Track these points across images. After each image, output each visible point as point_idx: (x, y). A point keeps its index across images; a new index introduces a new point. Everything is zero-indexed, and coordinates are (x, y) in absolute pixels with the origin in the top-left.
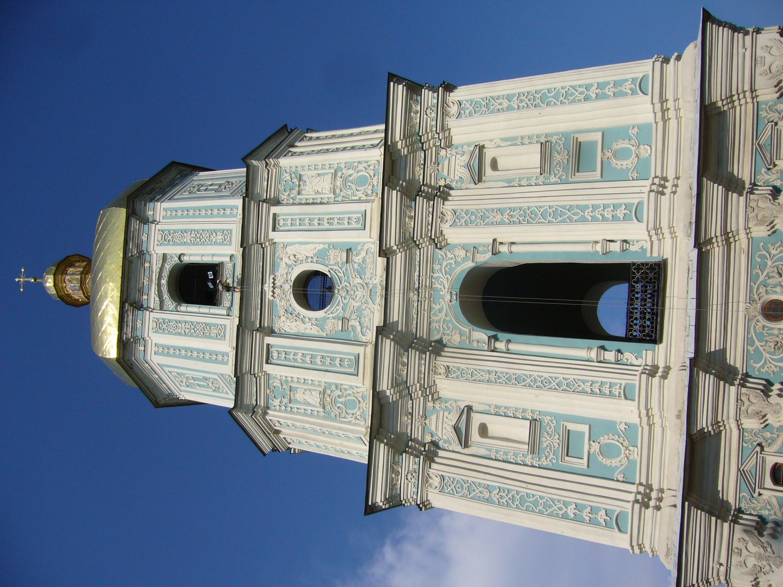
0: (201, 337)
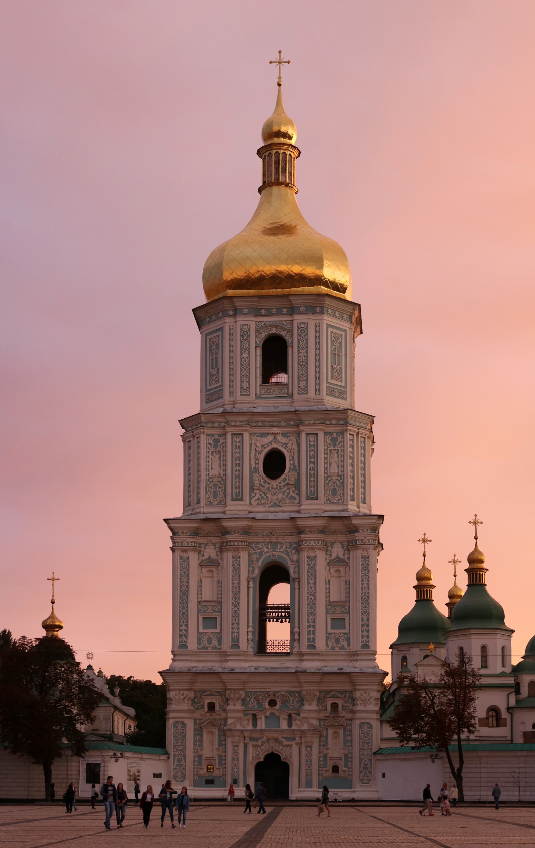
0: (241, 374)
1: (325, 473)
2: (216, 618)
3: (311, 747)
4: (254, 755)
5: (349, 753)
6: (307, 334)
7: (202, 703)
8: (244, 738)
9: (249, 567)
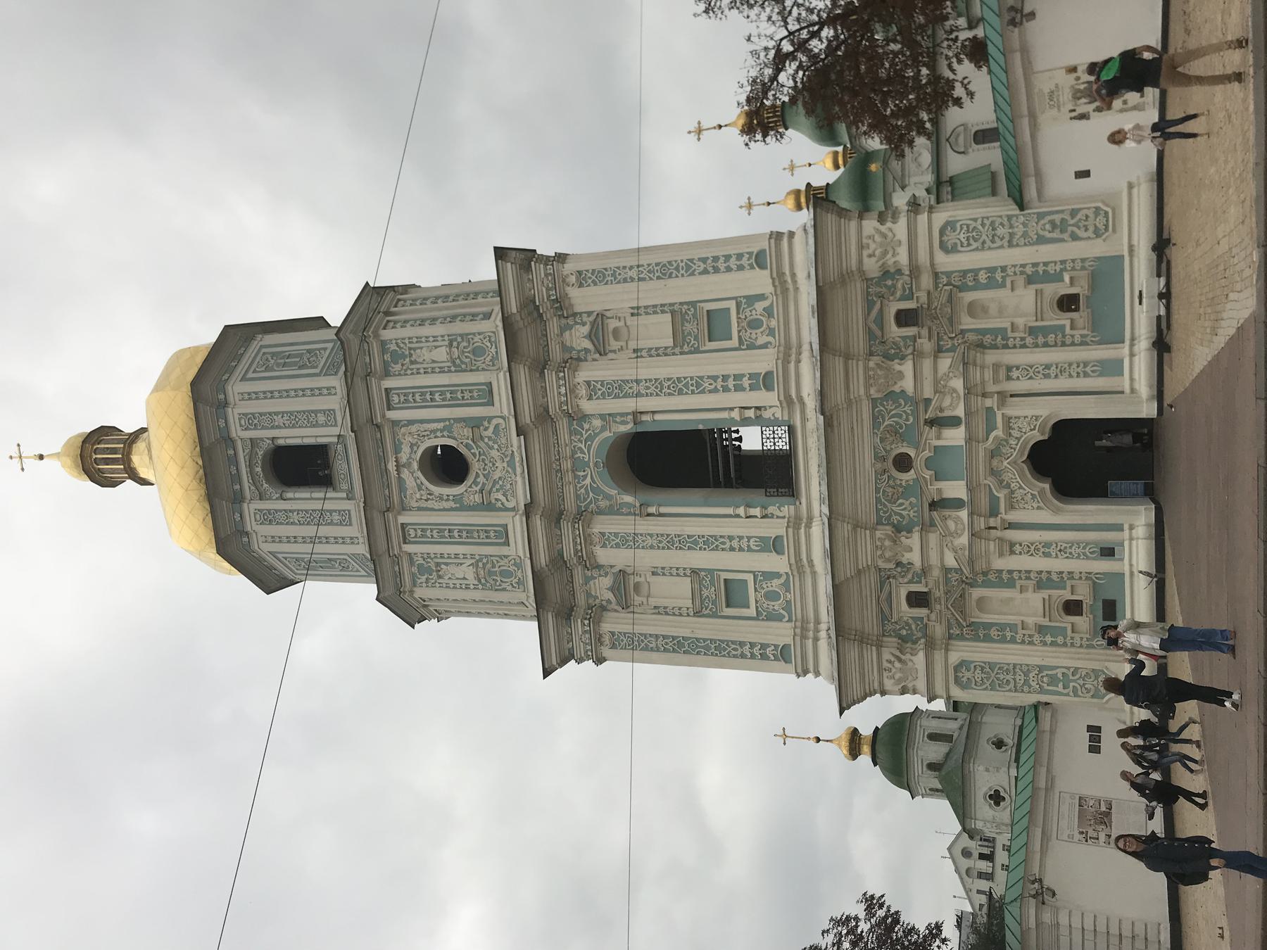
1: (450, 371)
2: (725, 580)
3: (1009, 369)
4: (1035, 505)
5: (1022, 273)
6: (253, 414)
7: (910, 621)
8: (990, 528)
9: (622, 514)
